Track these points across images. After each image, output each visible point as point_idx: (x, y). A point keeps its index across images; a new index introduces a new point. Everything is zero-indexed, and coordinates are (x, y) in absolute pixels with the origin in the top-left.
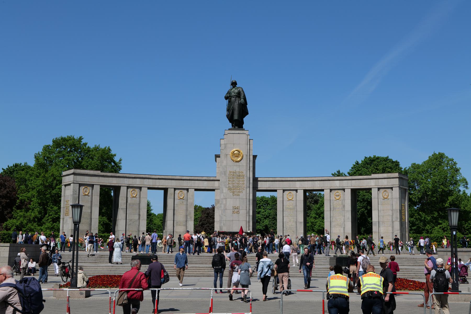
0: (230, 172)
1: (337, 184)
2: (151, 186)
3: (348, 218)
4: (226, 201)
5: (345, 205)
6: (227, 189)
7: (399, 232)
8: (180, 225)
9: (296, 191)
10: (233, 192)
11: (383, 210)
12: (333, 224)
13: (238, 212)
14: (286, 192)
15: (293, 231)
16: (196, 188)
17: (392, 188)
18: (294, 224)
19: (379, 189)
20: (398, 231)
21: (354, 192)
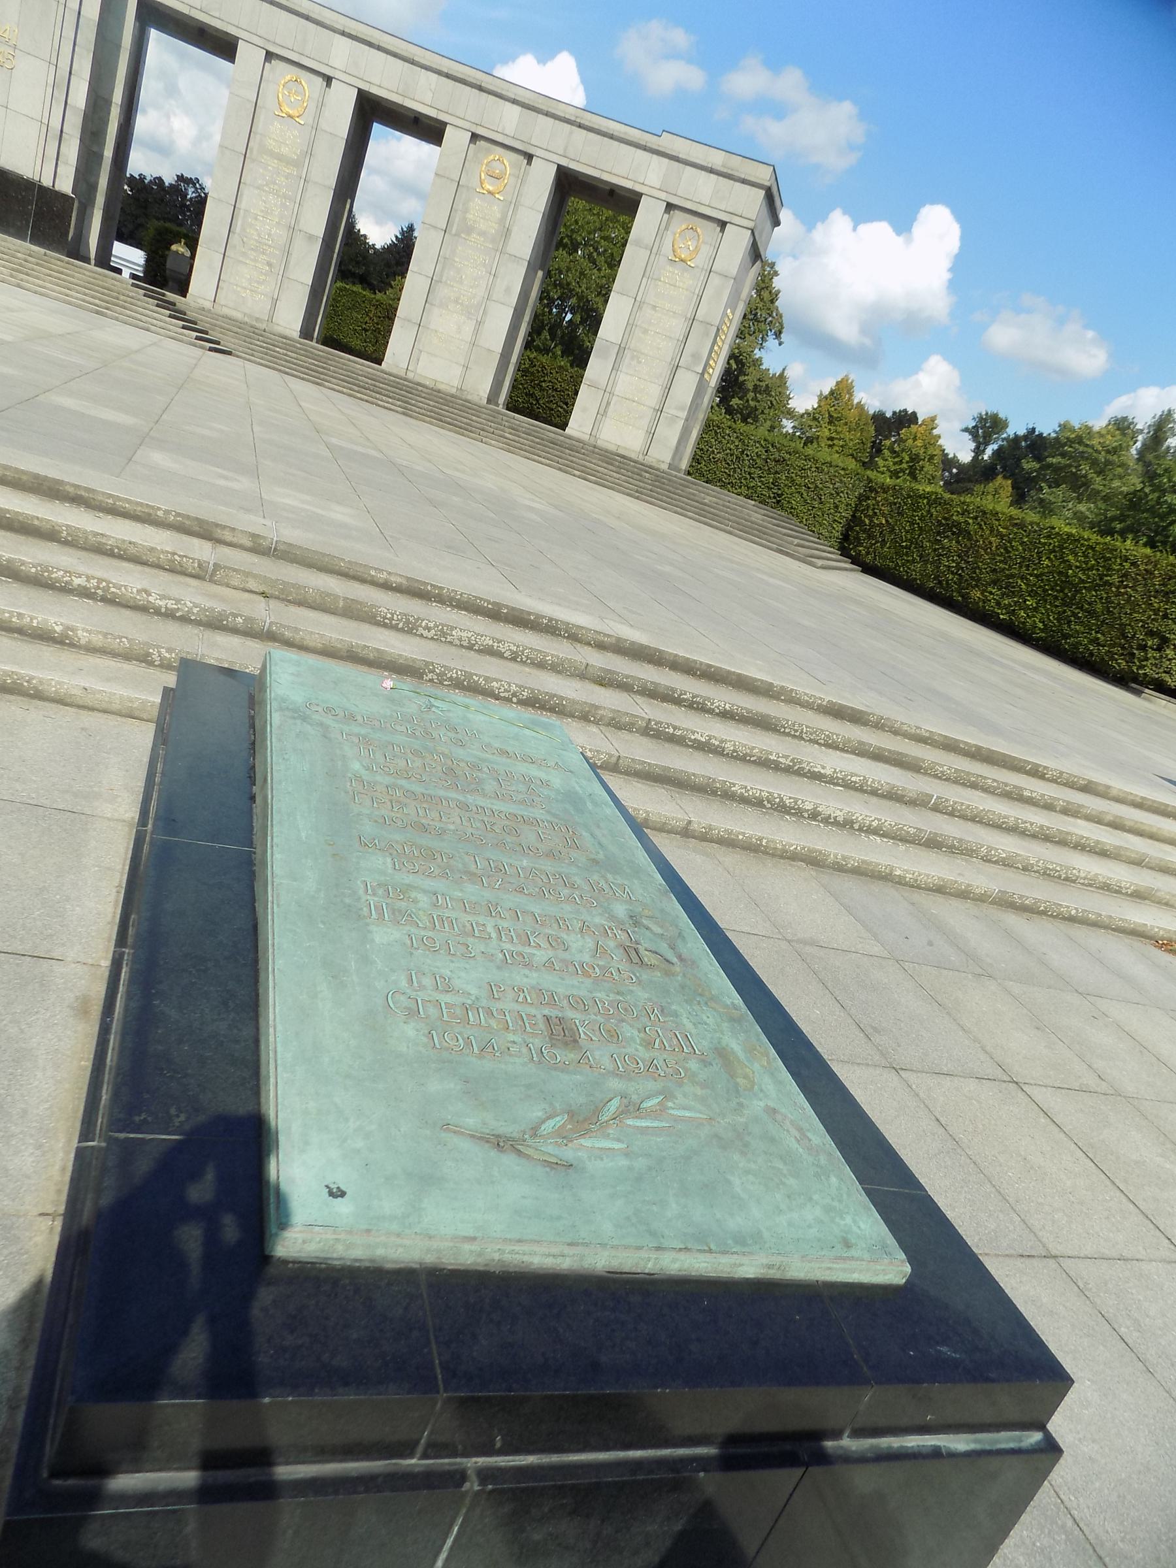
1: (507, 121)
3: (508, 290)
5: (515, 229)
7: (684, 415)
9: (328, 80)
11: (654, 307)
12: (442, 292)
15: (269, 264)
17: (723, 224)
18: (281, 234)
19: (670, 207)
20: (681, 409)
21: (568, 184)
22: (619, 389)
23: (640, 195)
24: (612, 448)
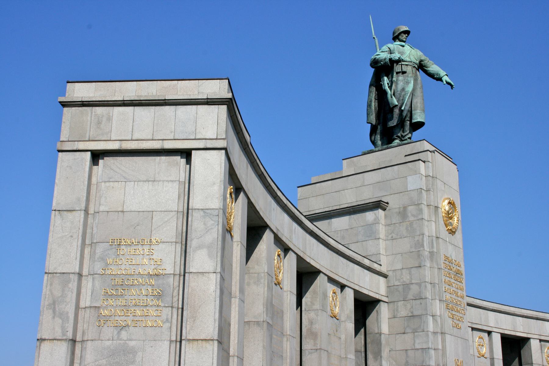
0: (447, 258)
4: (443, 341)
6: (444, 305)
9: (489, 333)
16: (357, 288)
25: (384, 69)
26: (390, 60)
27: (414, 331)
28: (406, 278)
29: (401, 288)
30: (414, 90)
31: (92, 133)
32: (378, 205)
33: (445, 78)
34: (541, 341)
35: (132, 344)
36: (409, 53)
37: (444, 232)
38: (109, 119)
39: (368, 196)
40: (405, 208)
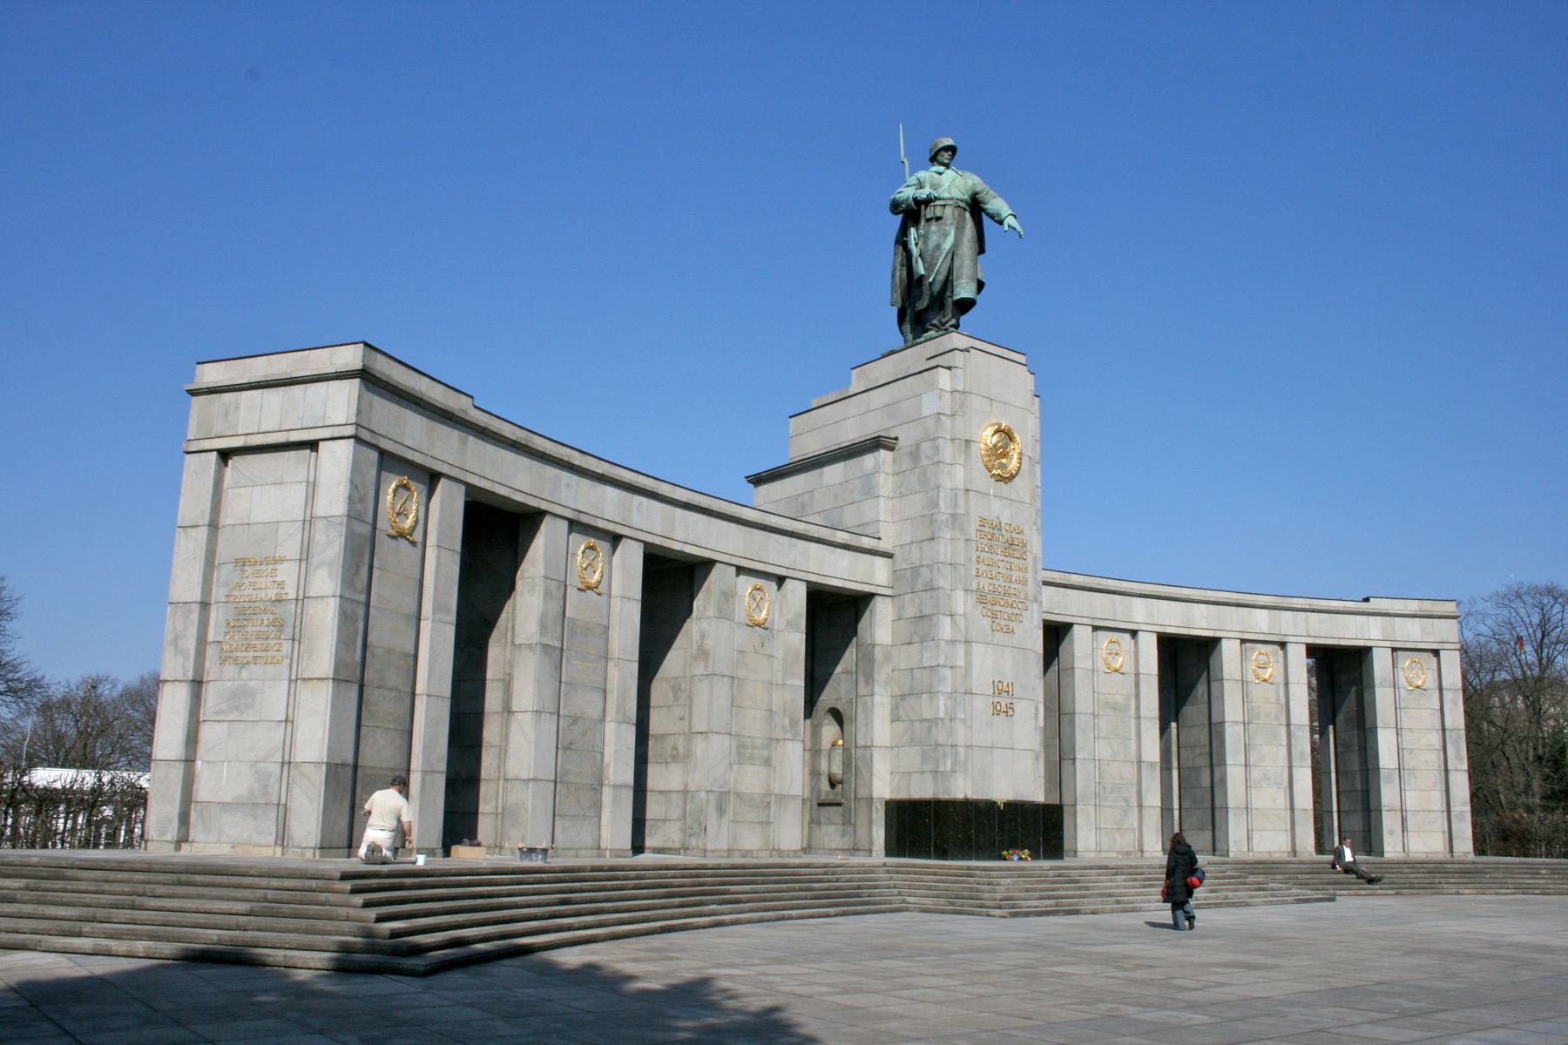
1: (1261, 623)
2: (658, 541)
4: (968, 654)
6: (972, 599)
8: (751, 758)
9: (1134, 633)
10: (994, 617)
11: (1411, 730)
12: (1255, 773)
13: (1009, 711)
14: (1101, 633)
15: (1126, 800)
18: (1130, 772)
22: (1410, 804)
23: (1369, 649)
24: (1422, 857)
25: (912, 213)
26: (915, 199)
27: (923, 640)
28: (915, 558)
29: (908, 573)
30: (956, 245)
31: (218, 428)
32: (876, 444)
33: (1011, 221)
34: (1243, 641)
35: (252, 684)
36: (952, 183)
37: (982, 480)
38: (237, 407)
39: (870, 429)
40: (918, 446)
